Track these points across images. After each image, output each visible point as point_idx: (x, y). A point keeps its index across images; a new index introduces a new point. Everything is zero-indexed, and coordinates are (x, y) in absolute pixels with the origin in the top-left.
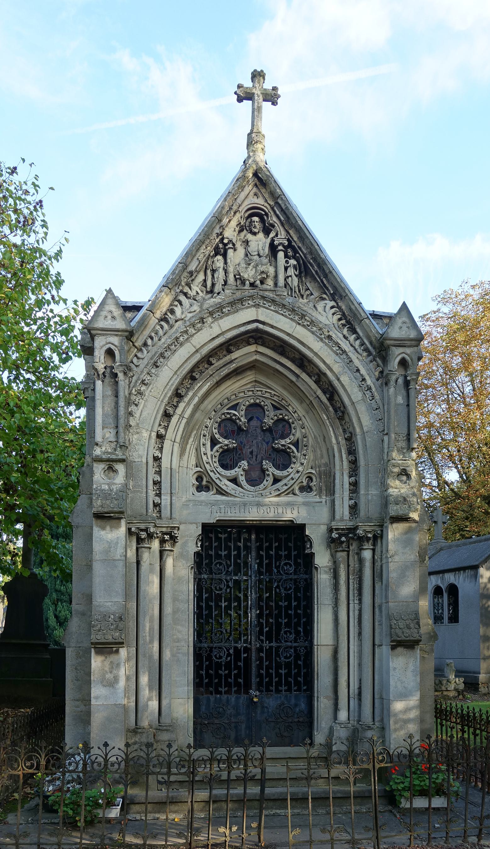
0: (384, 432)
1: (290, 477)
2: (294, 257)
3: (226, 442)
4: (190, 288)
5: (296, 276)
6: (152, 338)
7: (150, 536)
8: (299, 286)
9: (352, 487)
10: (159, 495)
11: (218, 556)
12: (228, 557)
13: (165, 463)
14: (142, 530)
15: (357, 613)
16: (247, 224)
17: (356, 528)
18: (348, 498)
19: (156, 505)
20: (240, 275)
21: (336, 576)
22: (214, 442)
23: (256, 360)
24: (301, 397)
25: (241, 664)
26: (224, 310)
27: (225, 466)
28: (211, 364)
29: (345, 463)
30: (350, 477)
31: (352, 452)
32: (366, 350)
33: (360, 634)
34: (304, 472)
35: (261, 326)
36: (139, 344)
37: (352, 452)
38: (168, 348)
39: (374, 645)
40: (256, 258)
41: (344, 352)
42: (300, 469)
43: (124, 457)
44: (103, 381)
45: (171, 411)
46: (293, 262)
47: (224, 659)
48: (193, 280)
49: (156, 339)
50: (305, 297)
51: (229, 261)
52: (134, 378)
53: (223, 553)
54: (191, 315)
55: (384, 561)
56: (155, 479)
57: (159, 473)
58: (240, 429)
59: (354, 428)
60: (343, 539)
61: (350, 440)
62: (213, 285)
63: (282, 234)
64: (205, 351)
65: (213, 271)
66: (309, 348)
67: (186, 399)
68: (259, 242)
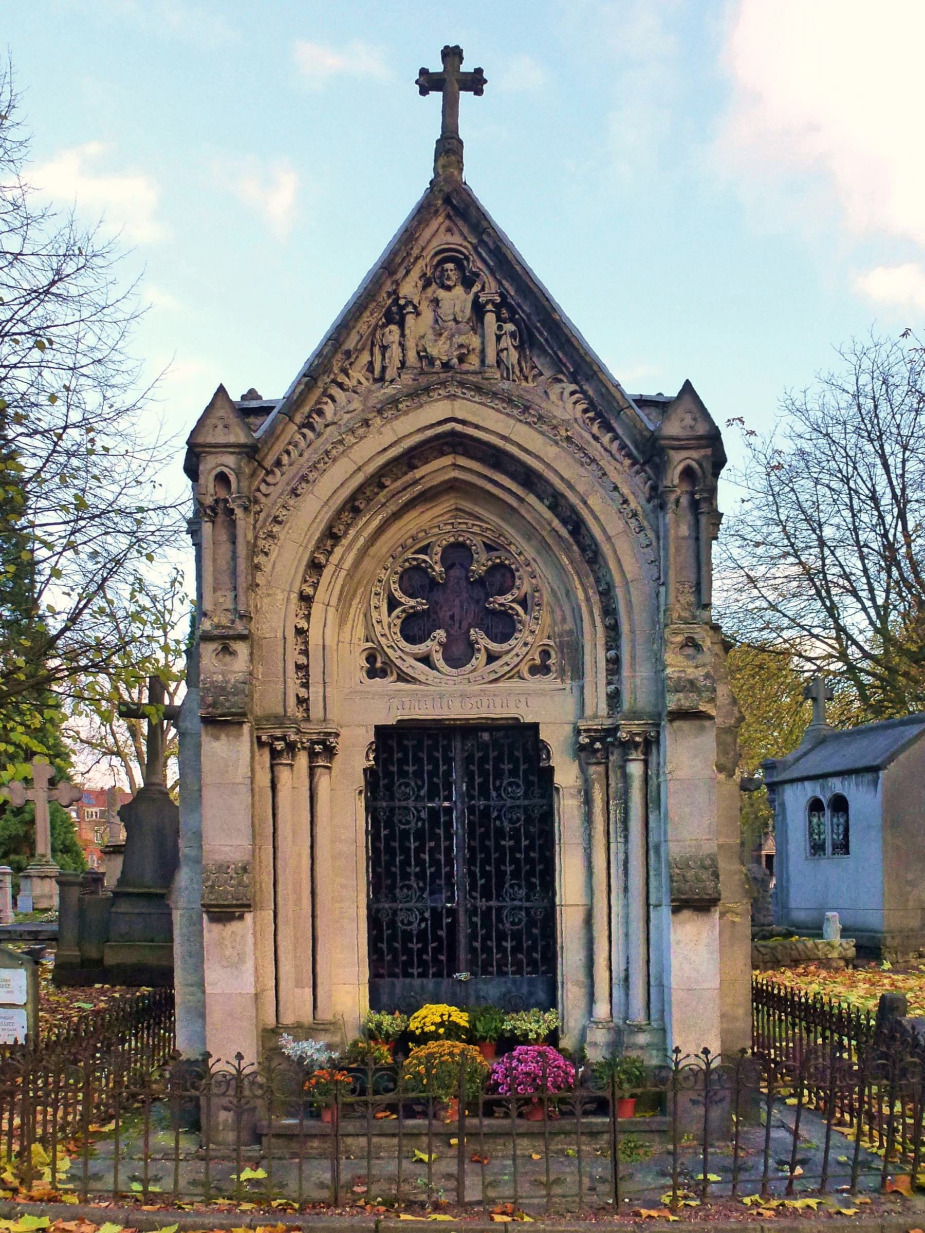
0: (660, 581)
1: (514, 652)
2: (512, 320)
3: (412, 602)
4: (348, 375)
5: (515, 347)
6: (288, 453)
7: (291, 747)
8: (519, 363)
9: (611, 666)
10: (306, 685)
11: (403, 774)
12: (418, 774)
13: (314, 637)
14: (278, 739)
15: (622, 856)
16: (437, 273)
17: (616, 728)
18: (604, 682)
19: (302, 701)
20: (425, 351)
21: (588, 801)
22: (393, 604)
23: (455, 479)
24: (530, 533)
25: (442, 933)
26: (400, 406)
27: (411, 639)
28: (382, 487)
29: (600, 629)
30: (608, 650)
31: (609, 611)
32: (629, 455)
33: (626, 889)
34: (537, 644)
35: (459, 427)
36: (269, 462)
37: (609, 611)
38: (314, 467)
39: (648, 905)
40: (452, 324)
41: (593, 461)
42: (530, 639)
43: (246, 632)
44: (213, 522)
45: (322, 559)
46: (510, 327)
47: (415, 925)
48: (351, 364)
49: (294, 453)
50: (530, 379)
51: (407, 331)
52: (262, 515)
53: (411, 769)
54: (348, 416)
55: (662, 779)
56: (299, 662)
57: (305, 653)
58: (433, 583)
59: (611, 576)
60: (598, 745)
61: (607, 594)
62: (384, 369)
63: (492, 285)
64: (371, 468)
65: (384, 349)
66: (537, 457)
67: (345, 542)
68: (457, 300)
